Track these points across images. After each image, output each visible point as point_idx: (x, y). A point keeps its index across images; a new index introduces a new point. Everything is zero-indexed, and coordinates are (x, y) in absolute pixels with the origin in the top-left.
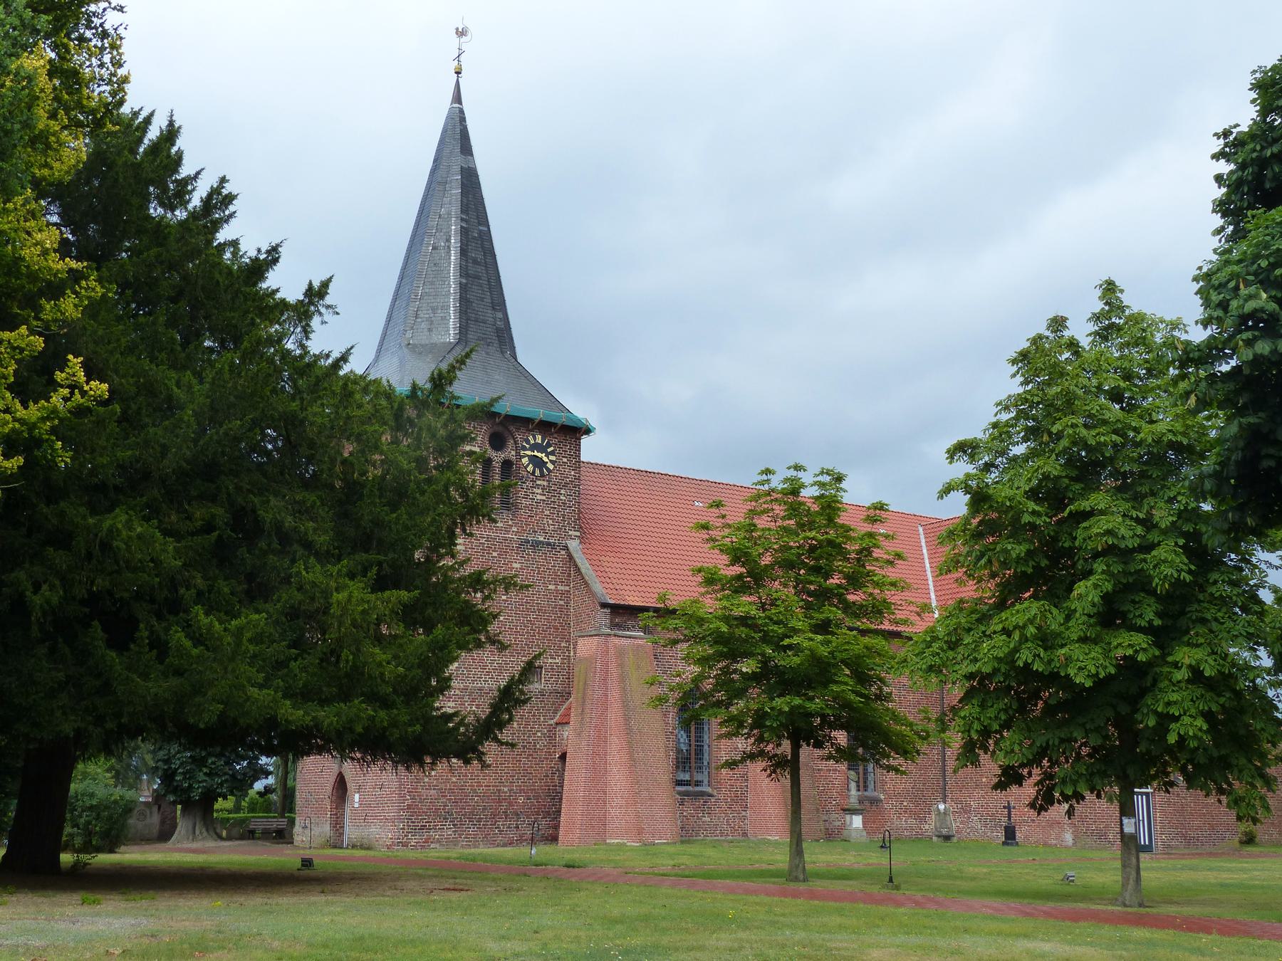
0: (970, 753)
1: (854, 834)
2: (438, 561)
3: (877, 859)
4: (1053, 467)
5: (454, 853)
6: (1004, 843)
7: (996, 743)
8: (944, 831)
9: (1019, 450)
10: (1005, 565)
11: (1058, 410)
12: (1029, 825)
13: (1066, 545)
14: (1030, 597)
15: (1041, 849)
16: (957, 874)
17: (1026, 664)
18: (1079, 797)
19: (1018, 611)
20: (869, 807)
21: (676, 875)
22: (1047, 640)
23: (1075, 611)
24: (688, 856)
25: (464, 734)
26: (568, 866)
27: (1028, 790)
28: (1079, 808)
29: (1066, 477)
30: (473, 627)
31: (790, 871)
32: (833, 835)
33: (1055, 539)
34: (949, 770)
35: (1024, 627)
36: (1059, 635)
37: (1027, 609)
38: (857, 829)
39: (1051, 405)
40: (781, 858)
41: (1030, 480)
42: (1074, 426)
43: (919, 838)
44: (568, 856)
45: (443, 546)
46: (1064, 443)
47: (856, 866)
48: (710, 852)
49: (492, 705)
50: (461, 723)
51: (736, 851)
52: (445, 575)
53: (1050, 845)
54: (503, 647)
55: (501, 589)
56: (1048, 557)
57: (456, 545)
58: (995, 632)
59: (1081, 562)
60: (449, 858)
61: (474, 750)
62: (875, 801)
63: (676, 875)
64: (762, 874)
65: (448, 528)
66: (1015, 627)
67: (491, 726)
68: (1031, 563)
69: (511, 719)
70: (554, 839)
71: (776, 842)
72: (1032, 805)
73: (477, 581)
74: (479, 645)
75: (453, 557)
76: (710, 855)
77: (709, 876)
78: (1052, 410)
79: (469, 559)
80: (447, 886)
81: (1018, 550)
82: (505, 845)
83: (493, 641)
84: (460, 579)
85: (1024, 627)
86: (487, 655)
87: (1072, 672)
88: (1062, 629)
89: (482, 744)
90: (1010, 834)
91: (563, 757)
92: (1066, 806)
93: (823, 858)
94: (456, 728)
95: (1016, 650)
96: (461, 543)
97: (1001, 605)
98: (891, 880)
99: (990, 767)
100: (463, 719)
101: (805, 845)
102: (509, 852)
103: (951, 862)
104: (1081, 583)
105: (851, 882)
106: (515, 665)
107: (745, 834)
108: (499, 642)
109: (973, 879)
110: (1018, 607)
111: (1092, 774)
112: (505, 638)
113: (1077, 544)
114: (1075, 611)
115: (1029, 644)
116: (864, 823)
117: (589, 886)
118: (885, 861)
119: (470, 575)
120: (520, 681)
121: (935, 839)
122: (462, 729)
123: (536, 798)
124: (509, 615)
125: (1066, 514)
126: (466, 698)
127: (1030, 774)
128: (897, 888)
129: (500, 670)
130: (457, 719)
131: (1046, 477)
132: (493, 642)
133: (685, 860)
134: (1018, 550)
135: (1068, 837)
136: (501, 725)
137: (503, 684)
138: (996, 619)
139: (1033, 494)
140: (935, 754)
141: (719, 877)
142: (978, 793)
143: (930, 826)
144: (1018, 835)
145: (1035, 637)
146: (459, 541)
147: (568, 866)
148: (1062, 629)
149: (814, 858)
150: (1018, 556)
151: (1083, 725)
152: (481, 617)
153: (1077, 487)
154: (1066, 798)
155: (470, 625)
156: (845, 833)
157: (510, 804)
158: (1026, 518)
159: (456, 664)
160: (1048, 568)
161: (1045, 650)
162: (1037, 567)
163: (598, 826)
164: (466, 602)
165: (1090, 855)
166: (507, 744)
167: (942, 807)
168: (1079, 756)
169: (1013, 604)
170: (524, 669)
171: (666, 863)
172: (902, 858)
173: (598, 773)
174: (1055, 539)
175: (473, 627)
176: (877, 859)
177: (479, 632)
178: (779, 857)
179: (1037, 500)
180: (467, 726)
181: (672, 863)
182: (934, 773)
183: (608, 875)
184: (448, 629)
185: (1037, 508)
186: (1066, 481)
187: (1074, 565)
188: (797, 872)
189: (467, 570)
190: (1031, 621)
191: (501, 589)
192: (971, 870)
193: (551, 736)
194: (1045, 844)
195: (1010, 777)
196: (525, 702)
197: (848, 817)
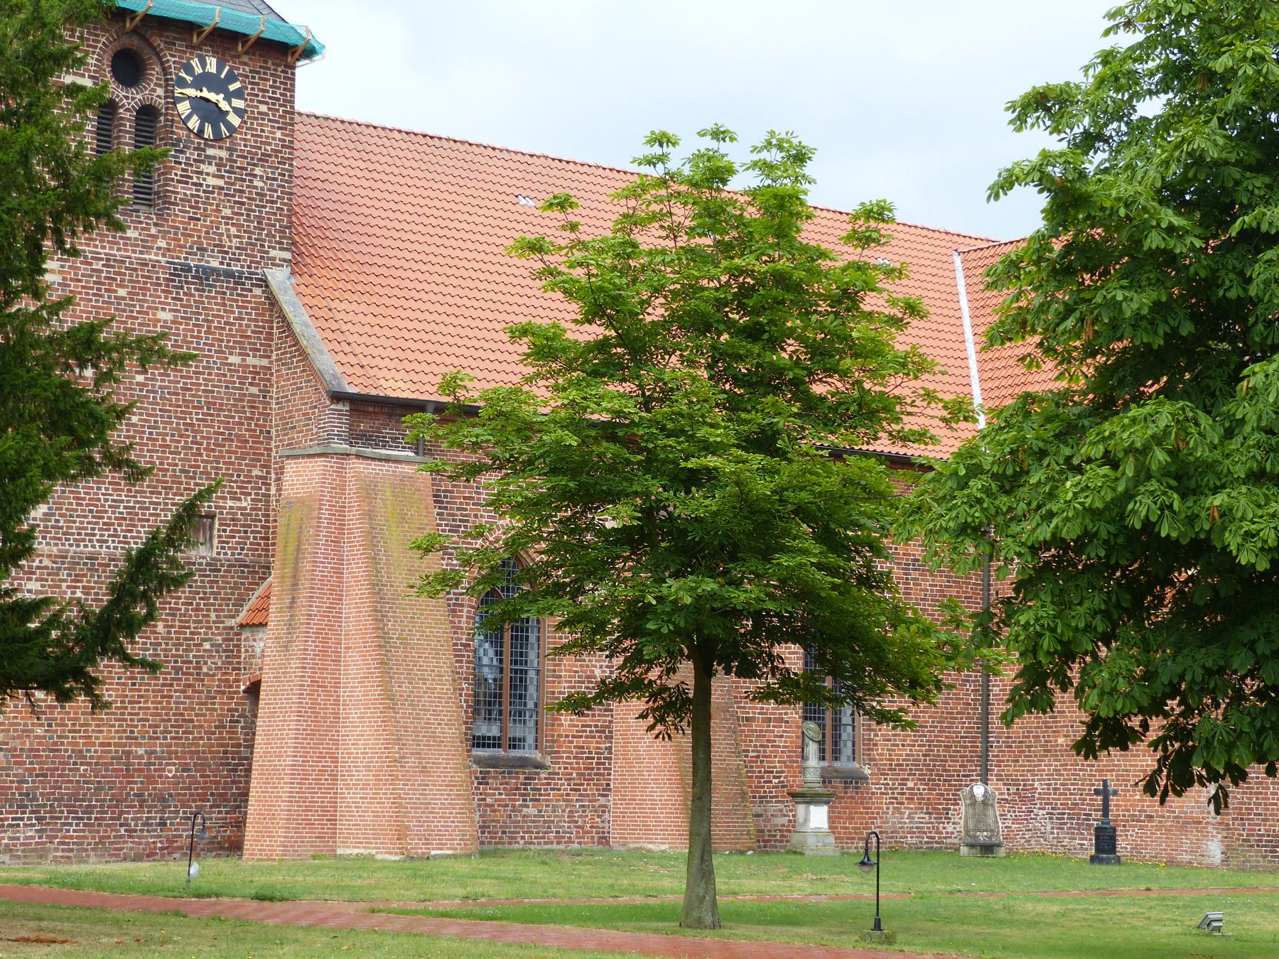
0: (1034, 692)
1: (811, 841)
2: (8, 303)
3: (853, 887)
4: (1210, 140)
5: (38, 872)
6: (1093, 859)
7: (1083, 672)
8: (983, 837)
9: (1151, 107)
10: (1115, 329)
11: (1228, 30)
12: (1146, 825)
13: (1232, 294)
14: (1158, 392)
15: (1162, 871)
16: (1002, 915)
17: (1148, 525)
18: (1239, 775)
19: (1134, 421)
20: (840, 788)
21: (469, 916)
22: (1188, 478)
23: (1242, 421)
24: (494, 880)
25: (58, 642)
26: (260, 898)
27: (1142, 759)
28: (1236, 794)
29: (1239, 163)
30: (77, 434)
31: (688, 909)
32: (772, 842)
33: (1211, 282)
34: (995, 720)
35: (1145, 450)
36: (1210, 467)
37: (1151, 418)
38: (817, 832)
39: (1217, 21)
40: (672, 885)
41: (1166, 163)
42: (1258, 59)
43: (934, 849)
44: (260, 879)
45: (17, 273)
46: (1237, 96)
47: (813, 899)
48: (535, 872)
49: (113, 588)
50: (54, 621)
51: (585, 871)
52: (21, 332)
53: (1179, 865)
54: (136, 474)
55: (131, 363)
56: (1195, 317)
57: (42, 272)
58: (1089, 461)
59: (1260, 327)
60: (28, 882)
61: (78, 674)
62: (853, 780)
63: (469, 916)
64: (636, 915)
65: (27, 239)
66: (1130, 450)
67: (111, 628)
68: (1162, 329)
69: (150, 616)
70: (234, 847)
71: (663, 856)
72: (1150, 788)
73: (85, 344)
74: (89, 468)
75: (37, 295)
76: (530, 877)
77: (533, 917)
78: (1216, 29)
79: (69, 301)
80: (24, 934)
81: (1137, 302)
82: (137, 858)
83: (117, 461)
84: (50, 340)
85: (1145, 450)
86: (105, 490)
87: (1232, 540)
88: (1217, 455)
89: (93, 662)
90: (1106, 843)
91: (254, 690)
92: (1212, 788)
93: (750, 884)
94: (42, 632)
95: (1129, 496)
96: (54, 271)
97: (1105, 406)
98: (878, 926)
99: (1069, 715)
100: (56, 616)
101: (717, 861)
102: (146, 871)
103: (993, 893)
104: (1257, 367)
105: (802, 930)
106: (160, 509)
107: (604, 840)
108: (128, 463)
109: (1033, 924)
110: (1134, 411)
111: (1261, 731)
112: (140, 457)
113: (1253, 291)
114: (1242, 421)
115: (1153, 485)
116: (832, 820)
117: (300, 935)
118: (868, 891)
119: (71, 333)
120: (170, 542)
121: (964, 850)
122: (54, 634)
123: (201, 767)
124: (148, 411)
125: (1234, 230)
126: (64, 574)
127: (1145, 726)
128: (890, 940)
129: (131, 519)
130: (46, 614)
131: (1198, 160)
132: (118, 464)
133: (488, 887)
134: (1137, 302)
135: (1214, 849)
136: (132, 627)
137: (136, 546)
138: (1092, 436)
139: (1171, 194)
140: (969, 693)
141: (552, 919)
142: (1049, 765)
143: (957, 824)
144: (1122, 844)
145: (1165, 472)
146: (49, 265)
147: (260, 898)
148: (1217, 455)
149: (734, 885)
150: (1138, 316)
151: (1251, 646)
152: (92, 414)
153: (1258, 182)
154: (1214, 776)
155: (71, 431)
156: (795, 838)
157: (150, 779)
158: (1154, 241)
159: (42, 509)
160: (1197, 339)
161: (1183, 497)
162: (1172, 335)
163: (321, 819)
164: (65, 385)
165: (1252, 880)
166: (143, 663)
167: (979, 790)
168: (1239, 696)
169: (1126, 407)
170: (179, 517)
171: (449, 893)
172: (900, 885)
173: (321, 721)
174: (1211, 282)
175: (77, 434)
176: (853, 887)
177: (90, 443)
178: (667, 883)
179: (1182, 207)
180: (64, 626)
181: (461, 892)
182: (966, 726)
183: (337, 915)
184: (27, 437)
185: (1177, 221)
186: (1236, 173)
187: (1247, 330)
188: (701, 908)
189: (68, 321)
190: (1158, 440)
191: (131, 363)
192: (1030, 908)
193: (231, 649)
194: (1171, 863)
195: (1107, 734)
196: (178, 582)
197: (801, 809)
